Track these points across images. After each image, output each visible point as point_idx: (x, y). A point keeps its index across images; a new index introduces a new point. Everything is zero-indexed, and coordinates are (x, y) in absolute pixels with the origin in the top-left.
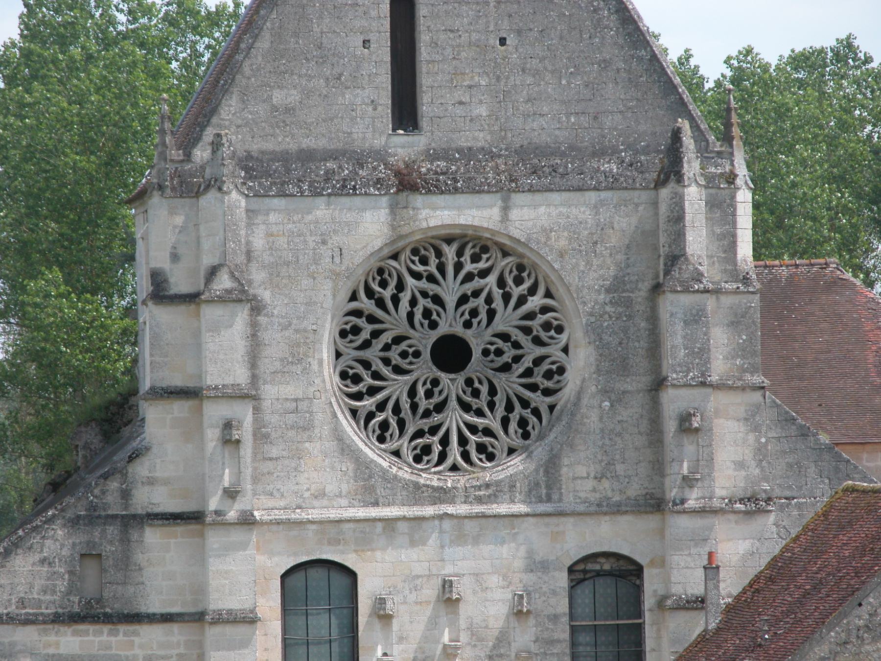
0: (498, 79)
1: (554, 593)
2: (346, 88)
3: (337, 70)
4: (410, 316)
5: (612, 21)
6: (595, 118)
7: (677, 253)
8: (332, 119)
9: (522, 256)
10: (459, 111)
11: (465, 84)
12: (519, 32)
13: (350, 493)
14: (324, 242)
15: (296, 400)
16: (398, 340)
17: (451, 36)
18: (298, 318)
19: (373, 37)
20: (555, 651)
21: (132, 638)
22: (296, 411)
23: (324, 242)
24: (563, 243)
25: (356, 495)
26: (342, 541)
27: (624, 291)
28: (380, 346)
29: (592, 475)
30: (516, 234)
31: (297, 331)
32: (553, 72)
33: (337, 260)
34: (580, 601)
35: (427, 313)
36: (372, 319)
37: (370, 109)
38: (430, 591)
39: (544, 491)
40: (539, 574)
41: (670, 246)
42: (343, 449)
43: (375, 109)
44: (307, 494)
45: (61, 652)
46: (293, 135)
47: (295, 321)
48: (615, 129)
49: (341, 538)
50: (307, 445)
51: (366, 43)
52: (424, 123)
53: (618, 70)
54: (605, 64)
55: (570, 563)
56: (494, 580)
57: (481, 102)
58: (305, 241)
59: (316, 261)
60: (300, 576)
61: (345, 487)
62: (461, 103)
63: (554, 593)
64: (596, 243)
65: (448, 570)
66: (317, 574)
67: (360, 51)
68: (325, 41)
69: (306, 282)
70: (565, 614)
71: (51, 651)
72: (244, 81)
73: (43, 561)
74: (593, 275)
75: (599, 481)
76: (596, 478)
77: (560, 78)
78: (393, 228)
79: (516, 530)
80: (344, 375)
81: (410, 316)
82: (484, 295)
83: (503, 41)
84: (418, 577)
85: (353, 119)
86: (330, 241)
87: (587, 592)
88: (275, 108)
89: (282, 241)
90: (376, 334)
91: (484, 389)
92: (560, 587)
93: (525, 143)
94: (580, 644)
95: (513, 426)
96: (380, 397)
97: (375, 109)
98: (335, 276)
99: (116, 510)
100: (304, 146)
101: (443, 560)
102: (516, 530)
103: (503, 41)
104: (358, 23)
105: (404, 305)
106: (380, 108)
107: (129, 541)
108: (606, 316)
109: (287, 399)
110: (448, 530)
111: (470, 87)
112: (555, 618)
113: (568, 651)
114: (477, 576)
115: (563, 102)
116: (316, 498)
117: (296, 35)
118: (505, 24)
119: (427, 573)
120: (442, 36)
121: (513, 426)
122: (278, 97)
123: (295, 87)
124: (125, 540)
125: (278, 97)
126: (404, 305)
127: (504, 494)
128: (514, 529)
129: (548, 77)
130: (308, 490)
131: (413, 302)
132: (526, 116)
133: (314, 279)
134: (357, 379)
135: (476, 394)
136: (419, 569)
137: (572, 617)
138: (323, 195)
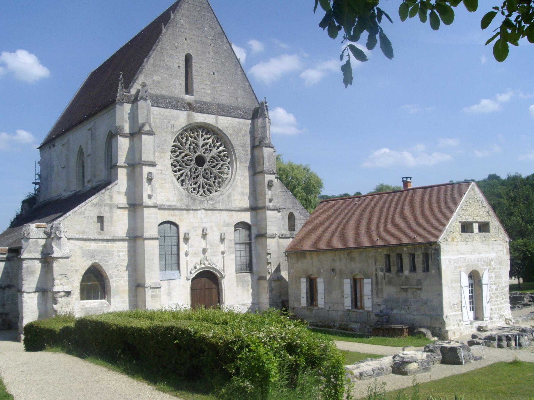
0: (213, 83)
2: (174, 79)
3: (171, 73)
4: (190, 149)
5: (240, 73)
6: (236, 99)
7: (264, 136)
8: (170, 87)
9: (218, 135)
10: (203, 91)
11: (205, 83)
12: (218, 72)
14: (169, 122)
15: (161, 170)
16: (186, 155)
17: (201, 69)
18: (162, 145)
19: (181, 65)
21: (114, 244)
22: (161, 174)
23: (169, 122)
24: (231, 132)
27: (246, 147)
28: (182, 157)
29: (239, 199)
30: (220, 127)
31: (161, 149)
32: (226, 84)
33: (173, 128)
35: (194, 149)
36: (179, 149)
37: (180, 86)
38: (200, 232)
39: (227, 203)
41: (261, 134)
42: (174, 187)
43: (181, 86)
44: (164, 200)
45: (91, 248)
46: (159, 90)
47: (161, 146)
48: (241, 103)
50: (165, 185)
51: (179, 66)
52: (194, 93)
53: (241, 87)
54: (238, 85)
55: (234, 224)
56: (216, 229)
57: (208, 89)
58: (164, 121)
59: (167, 128)
60: (162, 226)
61: (175, 199)
62: (203, 88)
64: (239, 133)
65: (204, 225)
66: (167, 226)
67: (177, 69)
68: (168, 64)
69: (164, 134)
71: (88, 248)
72: (146, 71)
73: (85, 217)
74: (238, 142)
77: (228, 86)
78: (188, 121)
80: (172, 165)
81: (190, 149)
82: (209, 145)
83: (214, 73)
84: (196, 227)
85: (175, 88)
86: (171, 123)
88: (154, 81)
89: (158, 121)
90: (180, 153)
91: (209, 173)
93: (219, 103)
95: (217, 184)
96: (182, 172)
97: (181, 86)
98: (172, 133)
99: (108, 201)
100: (162, 94)
101: (202, 222)
103: (214, 73)
104: (177, 61)
105: (188, 145)
106: (182, 86)
107: (112, 212)
108: (242, 154)
109: (158, 170)
111: (206, 84)
112: (231, 241)
114: (211, 227)
115: (229, 93)
116: (167, 201)
117: (160, 60)
118: (214, 69)
119: (198, 226)
120: (199, 69)
121: (217, 184)
122: (155, 78)
123: (160, 76)
124: (111, 212)
125: (155, 78)
126: (188, 145)
129: (225, 85)
130: (165, 199)
131: (190, 145)
132: (220, 95)
133: (166, 133)
134: (175, 166)
135: (207, 173)
136: (196, 225)
138: (169, 108)
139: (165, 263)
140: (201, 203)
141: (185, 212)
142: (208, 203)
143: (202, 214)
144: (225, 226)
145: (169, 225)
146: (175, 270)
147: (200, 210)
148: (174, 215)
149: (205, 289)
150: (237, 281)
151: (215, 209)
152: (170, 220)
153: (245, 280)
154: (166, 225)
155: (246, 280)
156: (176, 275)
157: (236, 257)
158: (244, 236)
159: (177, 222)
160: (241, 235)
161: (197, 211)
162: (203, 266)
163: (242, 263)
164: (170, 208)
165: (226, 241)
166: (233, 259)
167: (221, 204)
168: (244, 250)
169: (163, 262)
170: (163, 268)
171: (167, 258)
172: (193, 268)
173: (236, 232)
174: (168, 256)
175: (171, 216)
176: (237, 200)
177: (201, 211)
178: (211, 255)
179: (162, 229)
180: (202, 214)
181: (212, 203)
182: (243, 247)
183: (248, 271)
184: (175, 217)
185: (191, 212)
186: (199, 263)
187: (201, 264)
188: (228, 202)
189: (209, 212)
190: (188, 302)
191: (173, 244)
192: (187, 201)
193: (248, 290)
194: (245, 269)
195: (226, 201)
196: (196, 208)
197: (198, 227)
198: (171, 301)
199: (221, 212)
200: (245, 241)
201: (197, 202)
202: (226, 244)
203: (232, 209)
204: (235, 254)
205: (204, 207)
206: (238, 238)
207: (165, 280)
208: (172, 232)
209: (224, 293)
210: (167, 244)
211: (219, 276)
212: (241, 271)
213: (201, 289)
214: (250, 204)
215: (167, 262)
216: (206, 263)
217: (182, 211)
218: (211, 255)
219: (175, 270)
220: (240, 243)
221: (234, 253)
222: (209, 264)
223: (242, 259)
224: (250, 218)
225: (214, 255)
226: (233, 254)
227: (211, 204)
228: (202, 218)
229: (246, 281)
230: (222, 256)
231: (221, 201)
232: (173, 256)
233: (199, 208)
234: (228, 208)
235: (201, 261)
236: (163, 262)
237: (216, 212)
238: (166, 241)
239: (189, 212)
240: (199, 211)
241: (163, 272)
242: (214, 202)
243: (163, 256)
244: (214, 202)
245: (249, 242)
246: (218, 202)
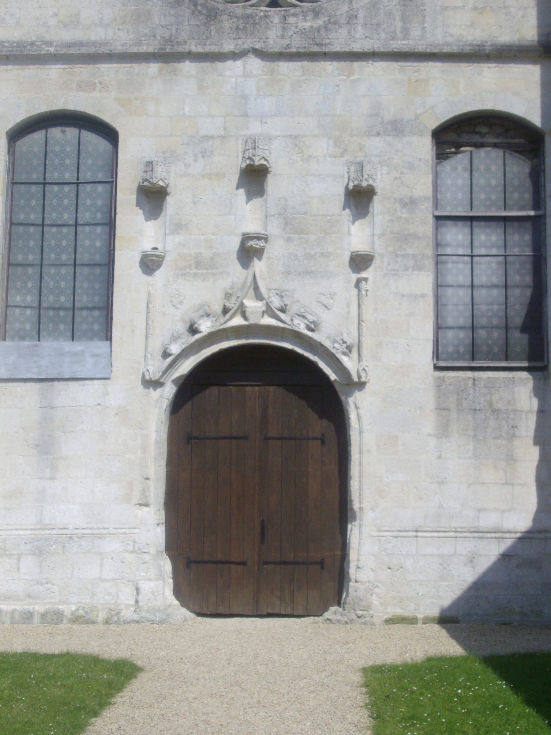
1: (411, 167)
13: (115, 20)
20: (410, 251)
25: (123, 23)
26: (98, 85)
29: (470, 5)
34: (449, 182)
39: (399, 25)
40: (388, 138)
44: (53, 22)
49: (96, 81)
55: (434, 124)
63: (411, 167)
70: (426, 198)
75: (480, 13)
76: (475, 9)
79: (356, 76)
87: (460, 168)
92: (420, 159)
94: (447, 245)
102: (356, 76)
110: (255, 72)
113: (429, 252)
116: (66, 26)
119: (222, 132)
127: (340, 27)
128: (353, 74)
137: (436, 203)
139: (36, 304)
140: (250, 28)
141: (154, 68)
142: (284, 28)
143: (246, 75)
144: (378, 134)
145: (71, 133)
146: (90, 336)
147: (235, 56)
148: (90, 86)
149: (267, 439)
150: (441, 408)
151: (316, 49)
152: (91, 111)
153: (491, 404)
154: (56, 132)
155: (499, 406)
156: (90, 361)
157: (438, 286)
158: (496, 181)
159: (106, 117)
160: (480, 180)
161: (219, 65)
162: (238, 321)
163: (484, 321)
164: (73, 51)
165: (377, 204)
166: (423, 296)
167: (360, 31)
168: (494, 252)
169: (29, 299)
170: (28, 326)
171: (49, 283)
172: (182, 328)
173: (447, 166)
174: (53, 271)
175: (80, 87)
176: (455, 8)
177: (239, 63)
178: (287, 273)
179: (38, 149)
180: (246, 75)
181: (307, 25)
182: (494, 238)
183: (525, 364)
184: (96, 94)
185: (188, 67)
186: (218, 309)
187: (225, 311)
188: (404, 19)
189: (284, 67)
190: (143, 492)
191: (85, 216)
192: (172, 19)
193: (511, 459)
194: (496, 349)
195: (390, 14)
196: (214, 49)
197: (223, 137)
198: (52, 478)
199: (356, 65)
200: (505, 207)
201: (227, 24)
202: (378, 219)
203: (420, 49)
204: (437, 274)
205: (258, 46)
206: (462, 196)
207: (25, 380)
208: (87, 161)
209: (360, 464)
210: (52, 216)
211: (333, 377)
212: (473, 359)
213: (245, 438)
214: (540, 26)
215: (49, 300)
216: (251, 304)
217: (137, 68)
218: (287, 273)
219: (91, 339)
220: (472, 219)
221: (430, 264)
222: (269, 311)
223: (477, 300)
224: (538, 102)
225: (309, 273)
226: (419, 268)
227: (302, 33)
228: (244, 98)
229: (496, 412)
230: (354, 277)
231: (361, 15)
232: (83, 271)
233: (228, 47)
234: (397, 45)
235: (228, 296)
236: (29, 299)
237: (330, 66)
238: (52, 202)
239: (175, 72)
240: (229, 63)
241: (26, 343)
242: (320, 22)
243: (30, 270)
244: (320, 22)
245: (532, 213)
246: (342, 21)
